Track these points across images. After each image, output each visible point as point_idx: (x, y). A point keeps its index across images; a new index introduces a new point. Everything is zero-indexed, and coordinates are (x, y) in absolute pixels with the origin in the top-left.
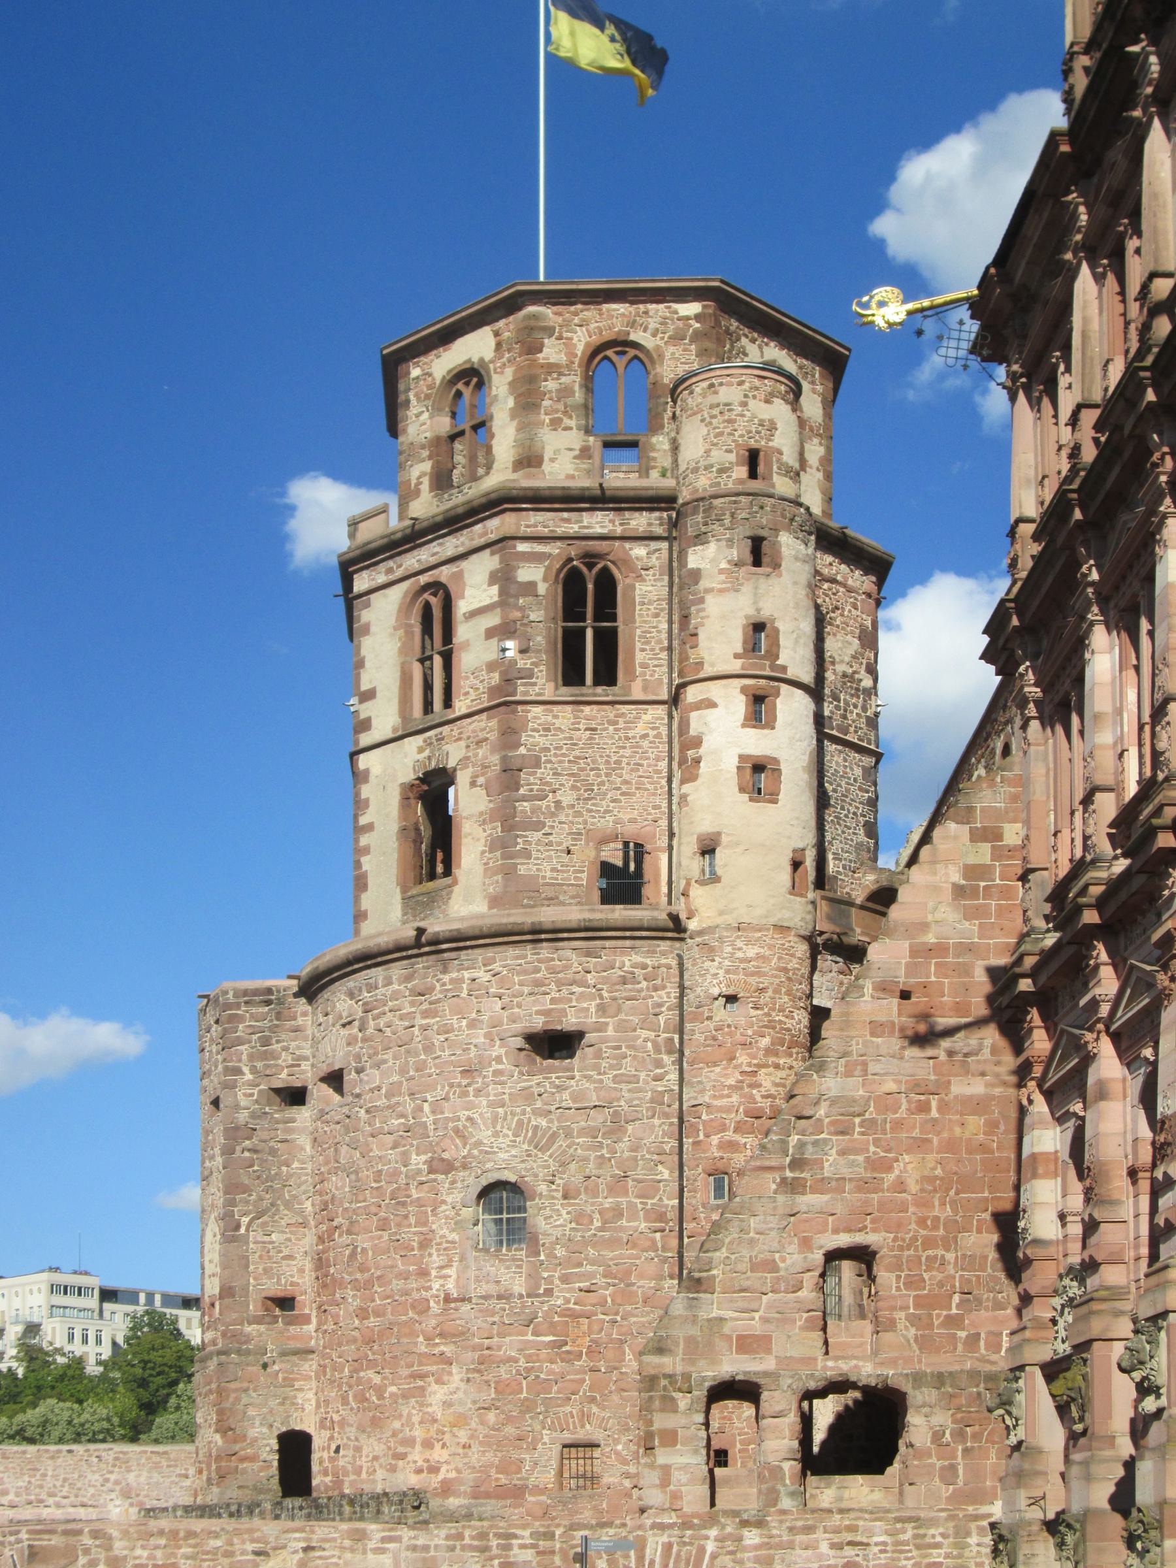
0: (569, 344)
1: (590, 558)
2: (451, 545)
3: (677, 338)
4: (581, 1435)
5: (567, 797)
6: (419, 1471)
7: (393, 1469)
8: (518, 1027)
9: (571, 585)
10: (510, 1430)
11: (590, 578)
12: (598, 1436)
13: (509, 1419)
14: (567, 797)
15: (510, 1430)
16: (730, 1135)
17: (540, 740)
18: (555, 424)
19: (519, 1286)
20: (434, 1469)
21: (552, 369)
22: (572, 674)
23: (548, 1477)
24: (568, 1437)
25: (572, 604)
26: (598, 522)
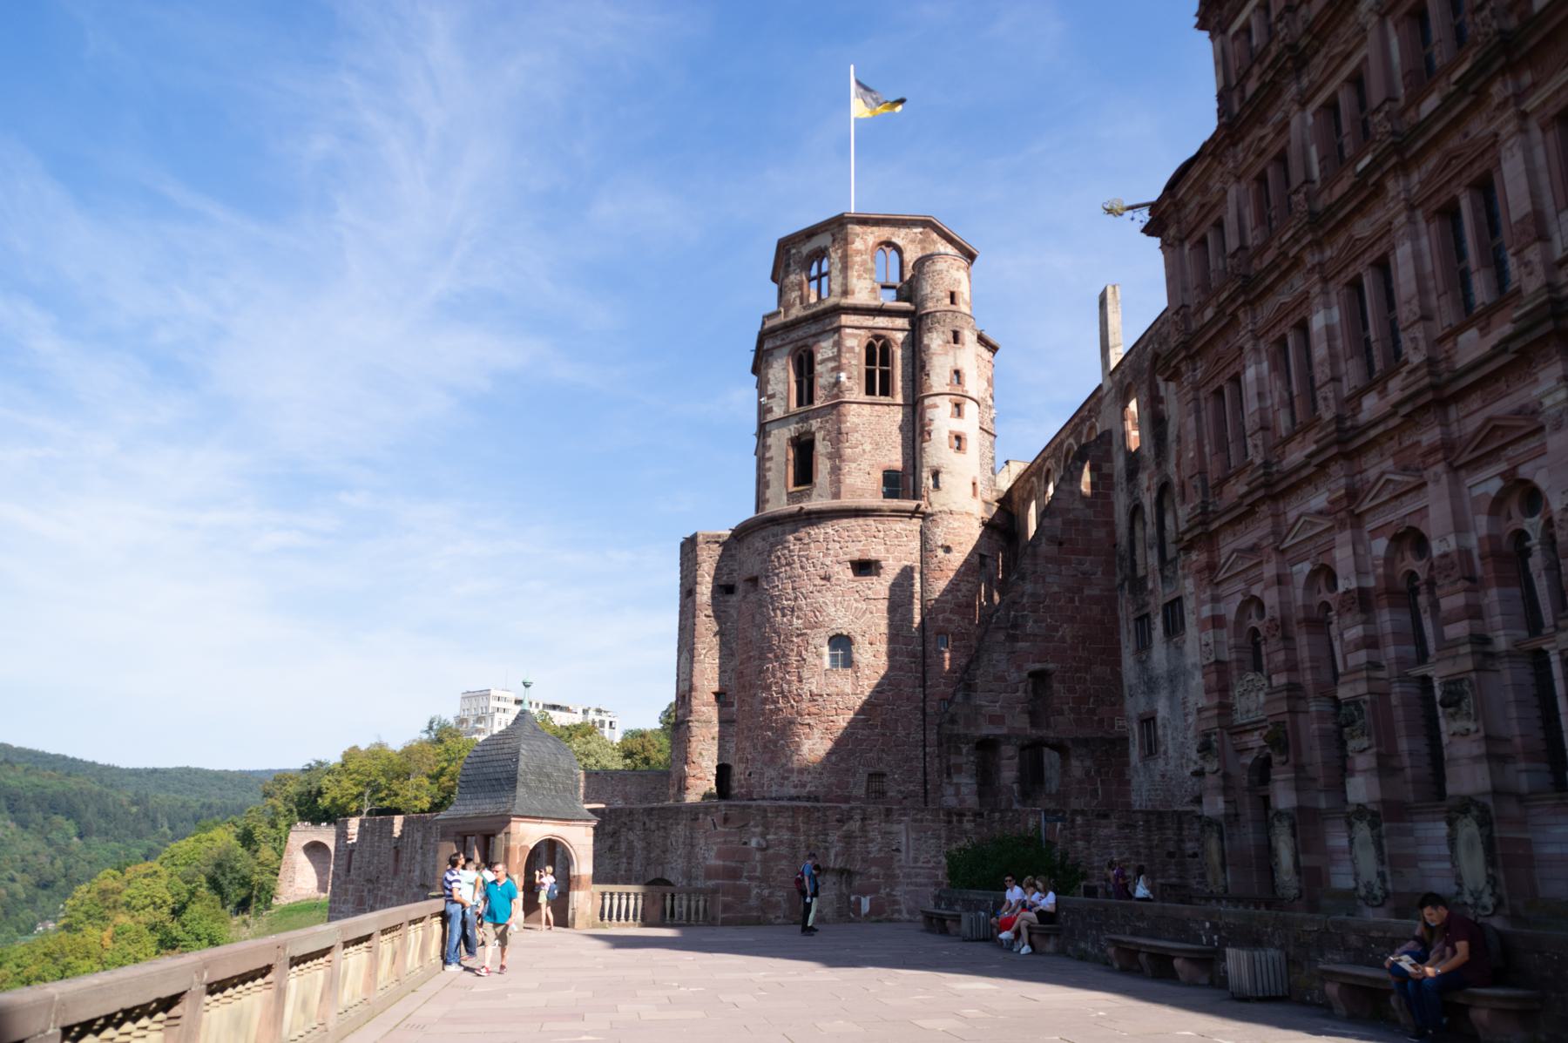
0: (865, 242)
1: (878, 337)
2: (814, 329)
3: (913, 241)
4: (878, 769)
5: (868, 447)
6: (795, 787)
7: (782, 785)
8: (848, 557)
9: (870, 349)
10: (843, 765)
11: (878, 345)
12: (886, 770)
13: (842, 759)
14: (868, 447)
15: (843, 765)
16: (947, 615)
17: (855, 420)
18: (859, 277)
19: (848, 689)
20: (804, 786)
21: (859, 252)
22: (870, 390)
23: (861, 792)
24: (871, 770)
25: (870, 359)
26: (881, 321)
